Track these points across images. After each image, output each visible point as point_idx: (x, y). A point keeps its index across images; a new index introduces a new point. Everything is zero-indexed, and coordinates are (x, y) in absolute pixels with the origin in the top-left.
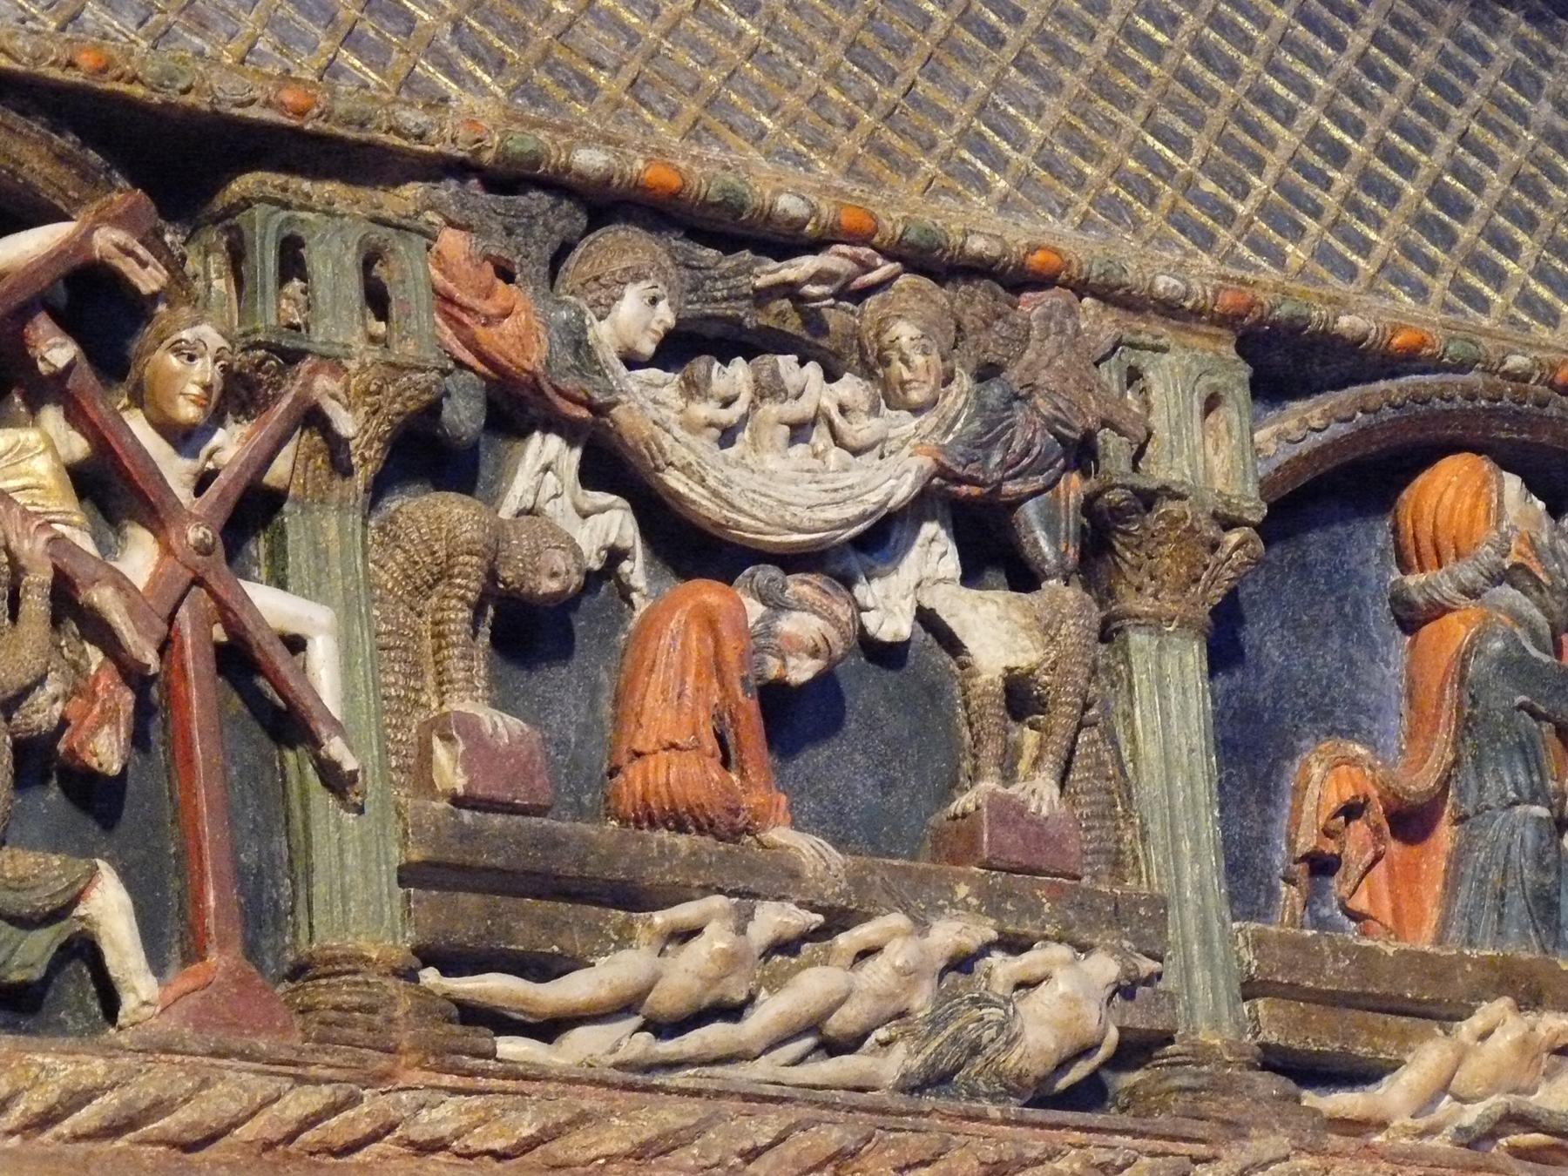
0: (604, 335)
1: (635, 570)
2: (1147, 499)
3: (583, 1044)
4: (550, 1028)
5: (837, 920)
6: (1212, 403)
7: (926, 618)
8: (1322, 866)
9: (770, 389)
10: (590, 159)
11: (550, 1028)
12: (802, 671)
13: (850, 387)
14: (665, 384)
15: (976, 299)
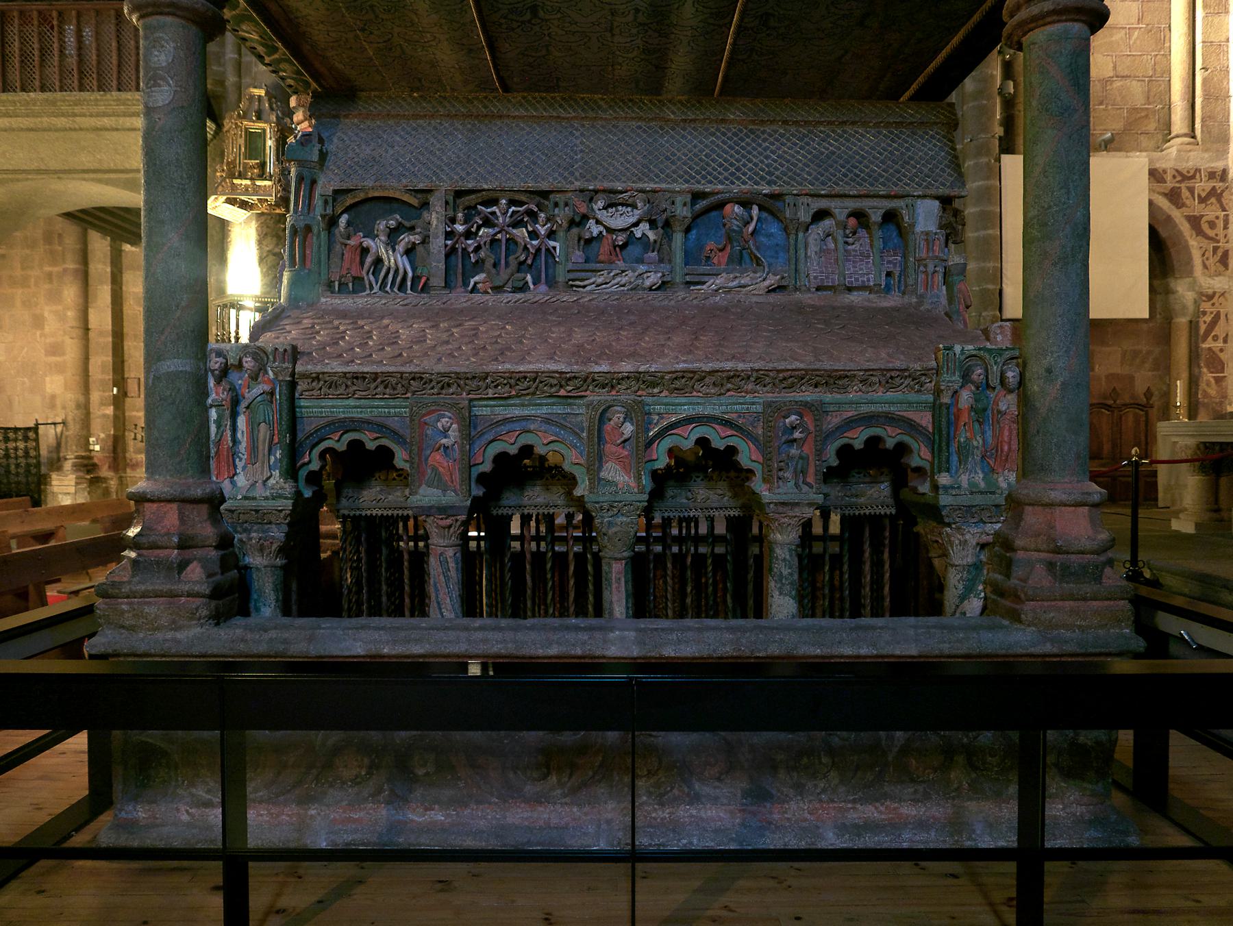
0: (595, 207)
1: (604, 233)
2: (674, 216)
3: (588, 288)
4: (584, 287)
5: (623, 272)
6: (685, 204)
7: (644, 234)
8: (708, 258)
9: (617, 211)
10: (591, 188)
11: (584, 287)
12: (621, 243)
13: (629, 209)
14: (605, 211)
15: (650, 196)
